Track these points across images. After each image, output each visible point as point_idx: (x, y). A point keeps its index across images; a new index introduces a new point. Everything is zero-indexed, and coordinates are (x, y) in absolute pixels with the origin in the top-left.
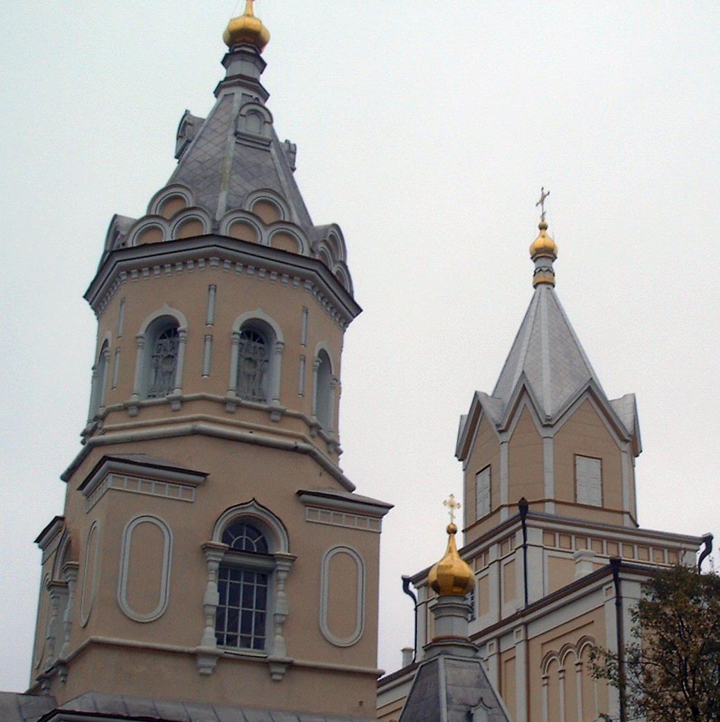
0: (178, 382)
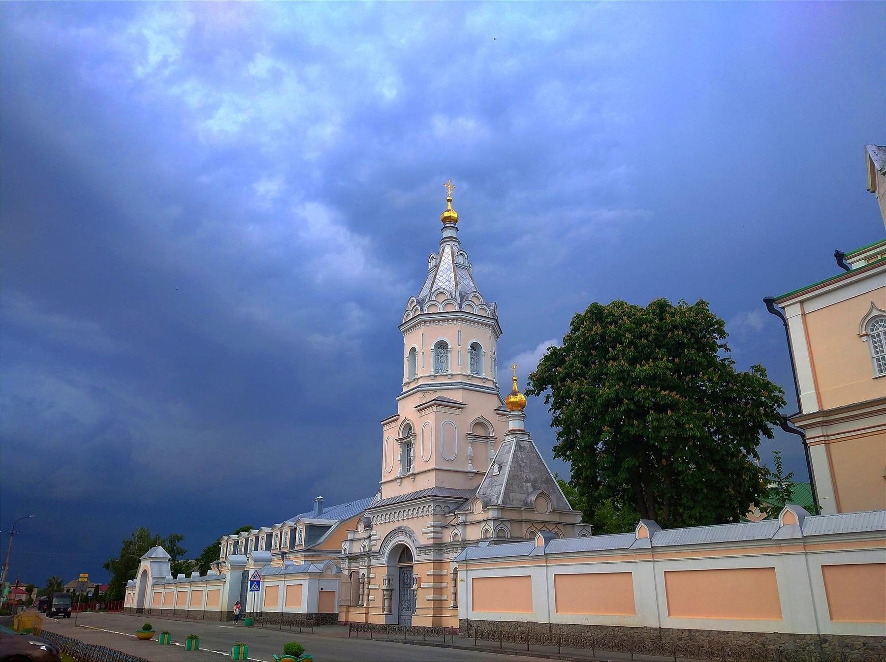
0: (449, 368)
